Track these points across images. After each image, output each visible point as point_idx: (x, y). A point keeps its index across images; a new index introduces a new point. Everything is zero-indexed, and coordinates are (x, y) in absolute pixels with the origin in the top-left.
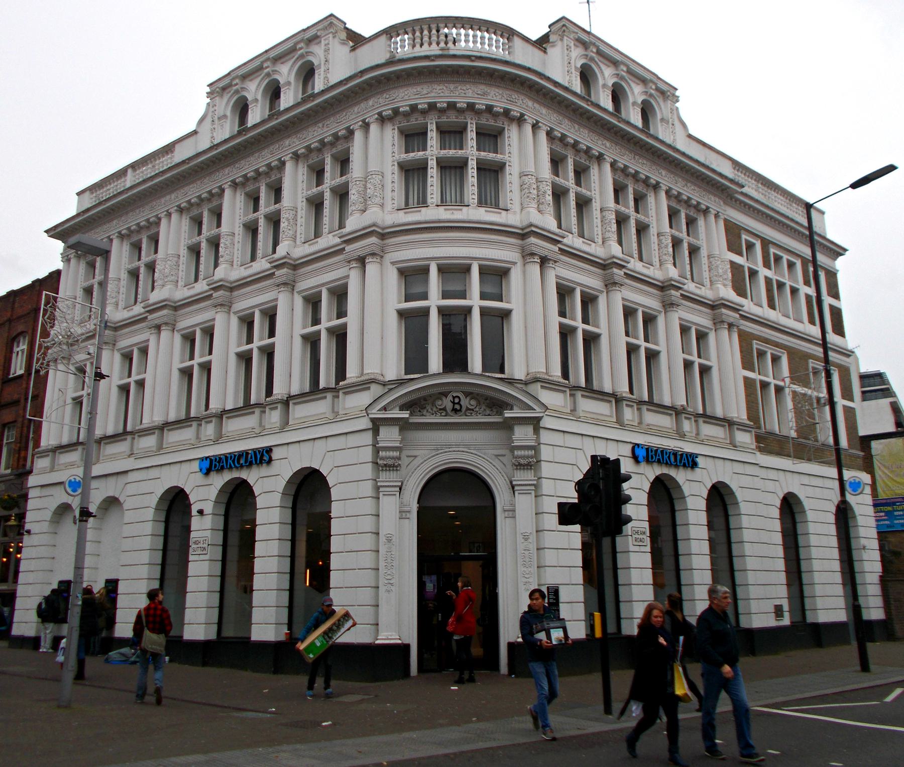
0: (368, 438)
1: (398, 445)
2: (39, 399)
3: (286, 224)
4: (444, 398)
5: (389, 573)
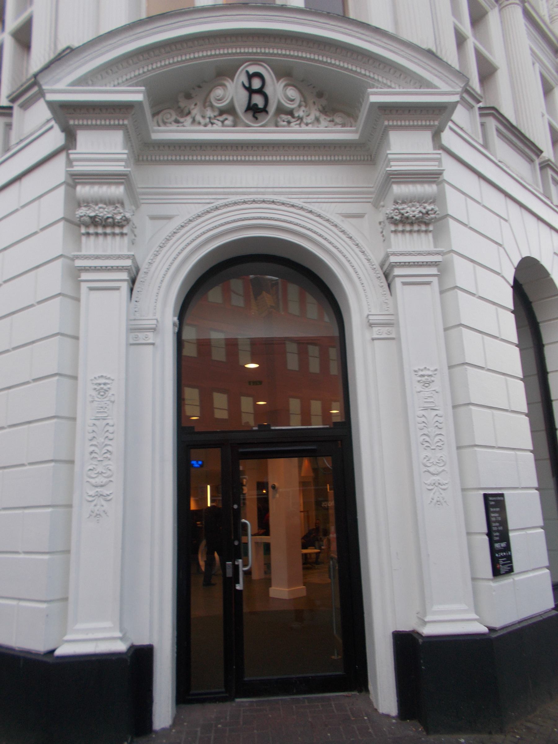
1: (119, 168)
4: (229, 84)
5: (100, 469)
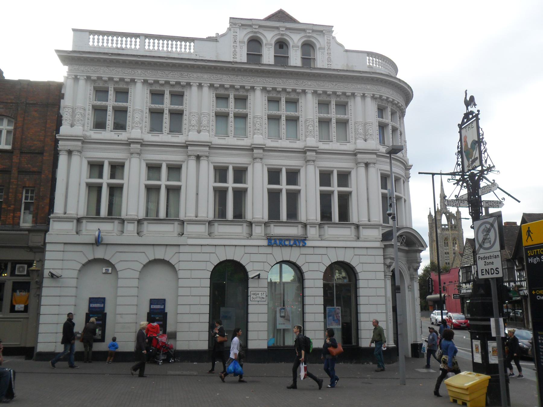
0: (381, 252)
2: (43, 176)
3: (312, 128)
